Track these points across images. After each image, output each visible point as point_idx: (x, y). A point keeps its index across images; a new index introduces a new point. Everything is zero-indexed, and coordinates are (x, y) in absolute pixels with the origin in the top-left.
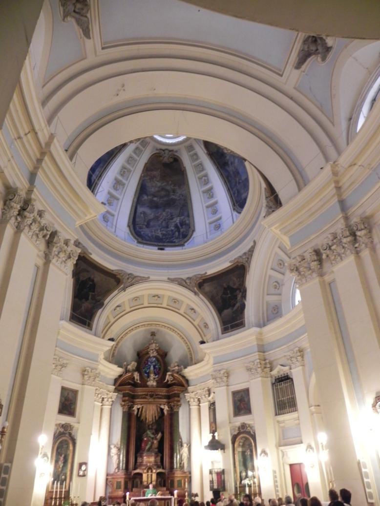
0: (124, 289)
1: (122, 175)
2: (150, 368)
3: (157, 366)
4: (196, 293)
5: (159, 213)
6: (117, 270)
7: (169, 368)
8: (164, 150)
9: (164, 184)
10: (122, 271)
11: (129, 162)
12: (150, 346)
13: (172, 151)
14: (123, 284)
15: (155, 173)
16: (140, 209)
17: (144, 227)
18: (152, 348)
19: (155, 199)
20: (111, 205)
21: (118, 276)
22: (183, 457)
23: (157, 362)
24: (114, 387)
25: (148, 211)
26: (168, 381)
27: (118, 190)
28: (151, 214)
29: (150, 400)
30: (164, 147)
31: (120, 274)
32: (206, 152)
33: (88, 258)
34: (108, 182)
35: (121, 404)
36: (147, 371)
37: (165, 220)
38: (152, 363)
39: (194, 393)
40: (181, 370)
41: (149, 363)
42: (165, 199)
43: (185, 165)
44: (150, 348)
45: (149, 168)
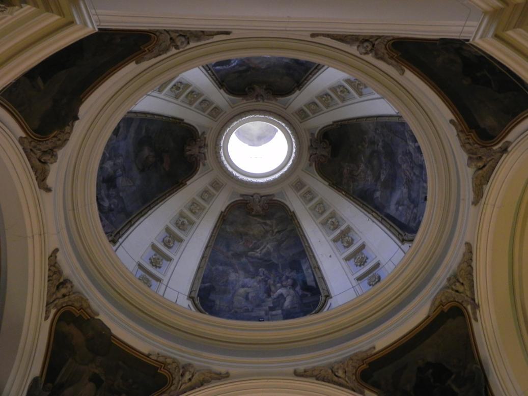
0: (476, 306)
1: (335, 228)
4: (504, 150)
5: (403, 175)
6: (431, 307)
8: (311, 156)
9: (362, 158)
10: (435, 299)
11: (320, 211)
13: (311, 140)
14: (465, 305)
15: (345, 171)
16: (392, 210)
17: (415, 210)
19: (383, 177)
20: (365, 262)
21: (446, 308)
25: (397, 196)
27: (353, 240)
28: (402, 191)
30: (306, 155)
31: (441, 304)
32: (298, 92)
33: (376, 357)
34: (330, 256)
37: (412, 168)
42: (383, 160)
43: (331, 123)
45: (337, 182)
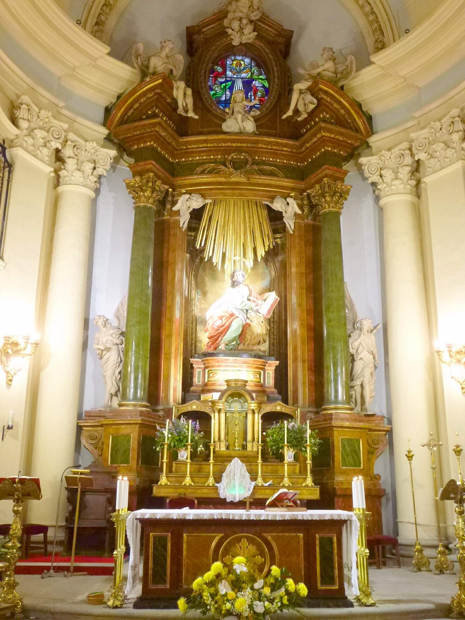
2: (231, 88)
3: (256, 83)
7: (301, 71)
12: (230, 8)
18: (239, 14)
22: (358, 366)
23: (255, 69)
24: (105, 131)
26: (297, 112)
29: (233, 179)
35: (128, 186)
36: (223, 98)
38: (240, 72)
39: (396, 151)
40: (346, 74)
41: (229, 74)
44: (230, 16)
